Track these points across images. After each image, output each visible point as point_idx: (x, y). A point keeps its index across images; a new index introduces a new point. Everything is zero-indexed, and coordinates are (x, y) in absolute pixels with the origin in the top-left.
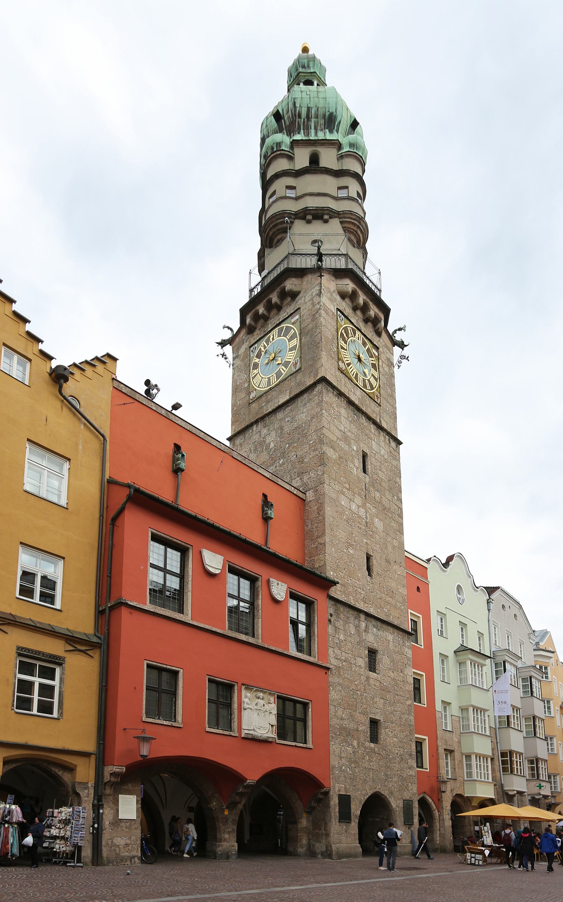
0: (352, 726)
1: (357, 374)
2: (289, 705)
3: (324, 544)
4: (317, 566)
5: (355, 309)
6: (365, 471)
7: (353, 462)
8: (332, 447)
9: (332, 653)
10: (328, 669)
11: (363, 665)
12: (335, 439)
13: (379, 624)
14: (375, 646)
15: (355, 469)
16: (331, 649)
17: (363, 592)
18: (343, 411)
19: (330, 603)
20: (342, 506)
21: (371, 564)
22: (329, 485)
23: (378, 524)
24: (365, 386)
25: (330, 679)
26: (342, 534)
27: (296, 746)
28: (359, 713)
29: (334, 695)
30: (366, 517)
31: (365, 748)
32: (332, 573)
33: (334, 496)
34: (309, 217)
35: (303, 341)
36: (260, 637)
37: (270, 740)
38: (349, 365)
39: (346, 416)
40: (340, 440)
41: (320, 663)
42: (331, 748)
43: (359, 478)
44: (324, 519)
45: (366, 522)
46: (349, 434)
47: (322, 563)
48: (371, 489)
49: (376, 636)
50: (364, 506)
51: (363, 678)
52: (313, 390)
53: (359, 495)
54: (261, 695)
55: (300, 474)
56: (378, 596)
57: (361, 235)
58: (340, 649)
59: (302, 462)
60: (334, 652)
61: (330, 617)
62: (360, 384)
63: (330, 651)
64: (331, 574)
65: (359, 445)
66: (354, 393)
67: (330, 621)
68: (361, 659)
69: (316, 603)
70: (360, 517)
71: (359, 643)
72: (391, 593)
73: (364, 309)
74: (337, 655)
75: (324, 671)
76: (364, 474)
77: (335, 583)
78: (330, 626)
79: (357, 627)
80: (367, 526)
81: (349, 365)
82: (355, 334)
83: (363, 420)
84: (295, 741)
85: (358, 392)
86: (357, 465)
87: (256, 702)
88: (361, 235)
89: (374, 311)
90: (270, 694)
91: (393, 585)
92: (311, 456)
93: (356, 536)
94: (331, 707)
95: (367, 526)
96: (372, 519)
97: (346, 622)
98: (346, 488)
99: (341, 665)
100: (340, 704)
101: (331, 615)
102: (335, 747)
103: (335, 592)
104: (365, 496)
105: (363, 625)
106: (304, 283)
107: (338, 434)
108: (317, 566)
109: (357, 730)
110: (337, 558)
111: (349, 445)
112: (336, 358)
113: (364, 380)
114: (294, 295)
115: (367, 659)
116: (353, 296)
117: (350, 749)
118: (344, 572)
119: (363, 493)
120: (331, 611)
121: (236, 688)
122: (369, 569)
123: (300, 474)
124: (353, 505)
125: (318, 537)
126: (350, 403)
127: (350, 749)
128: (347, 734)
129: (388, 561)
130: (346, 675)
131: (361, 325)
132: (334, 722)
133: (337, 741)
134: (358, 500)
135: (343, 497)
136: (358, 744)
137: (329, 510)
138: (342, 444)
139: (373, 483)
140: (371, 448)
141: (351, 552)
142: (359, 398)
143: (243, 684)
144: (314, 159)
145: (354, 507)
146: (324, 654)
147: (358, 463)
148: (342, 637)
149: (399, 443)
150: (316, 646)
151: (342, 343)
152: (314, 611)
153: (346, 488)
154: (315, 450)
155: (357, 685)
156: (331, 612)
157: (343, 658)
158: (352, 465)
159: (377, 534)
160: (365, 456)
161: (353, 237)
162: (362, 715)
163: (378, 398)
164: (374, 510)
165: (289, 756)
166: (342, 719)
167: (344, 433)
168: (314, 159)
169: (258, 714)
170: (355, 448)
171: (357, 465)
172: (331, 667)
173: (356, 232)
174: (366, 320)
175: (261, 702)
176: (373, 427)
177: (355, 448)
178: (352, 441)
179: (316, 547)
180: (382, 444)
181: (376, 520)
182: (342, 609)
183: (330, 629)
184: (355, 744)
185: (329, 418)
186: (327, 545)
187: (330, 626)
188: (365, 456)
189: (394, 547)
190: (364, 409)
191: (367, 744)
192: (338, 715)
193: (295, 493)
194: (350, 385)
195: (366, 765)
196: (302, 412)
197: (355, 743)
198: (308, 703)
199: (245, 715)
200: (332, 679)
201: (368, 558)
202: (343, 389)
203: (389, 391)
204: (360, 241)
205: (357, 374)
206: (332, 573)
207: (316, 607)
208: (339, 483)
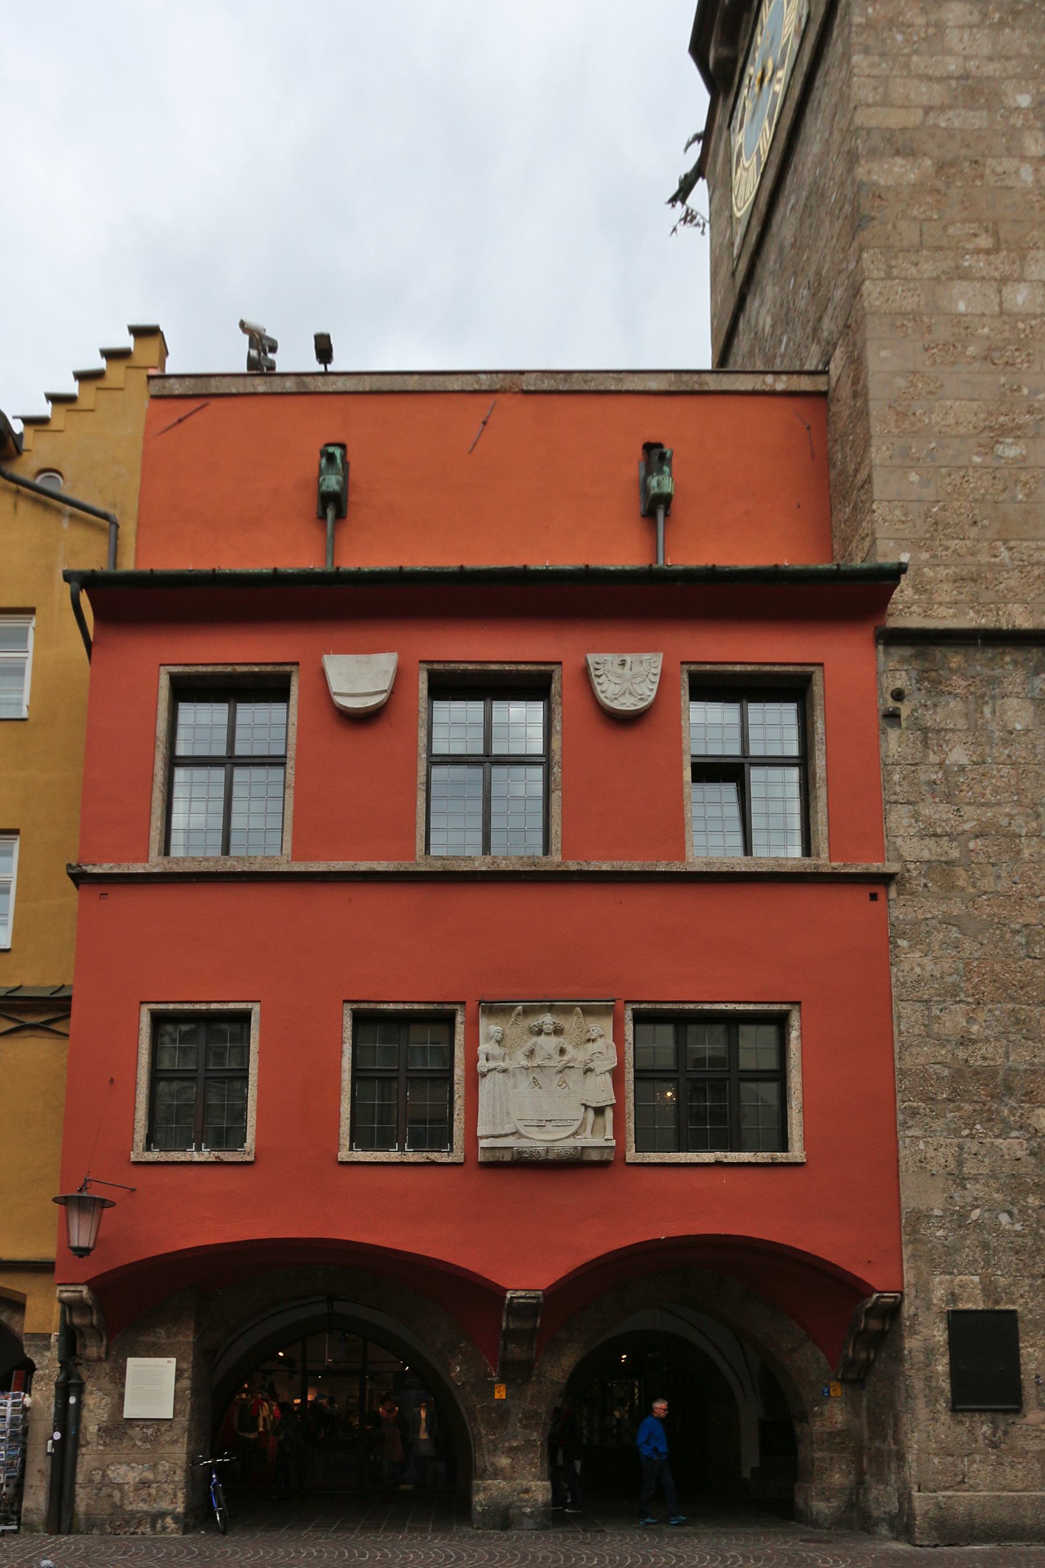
8: (898, 152)
9: (906, 822)
16: (904, 810)
22: (889, 276)
27: (718, 1164)
37: (595, 1156)
40: (942, 108)
42: (903, 1152)
58: (948, 798)
61: (891, 704)
67: (893, 716)
74: (932, 825)
75: (859, 895)
87: (528, 1046)
90: (587, 1012)
99: (955, 854)
103: (907, 610)
107: (936, 94)
120: (901, 680)
133: (938, 1125)
148: (958, 755)
152: (812, 707)
156: (899, 684)
157: (967, 827)
169: (535, 1081)
175: (548, 1043)
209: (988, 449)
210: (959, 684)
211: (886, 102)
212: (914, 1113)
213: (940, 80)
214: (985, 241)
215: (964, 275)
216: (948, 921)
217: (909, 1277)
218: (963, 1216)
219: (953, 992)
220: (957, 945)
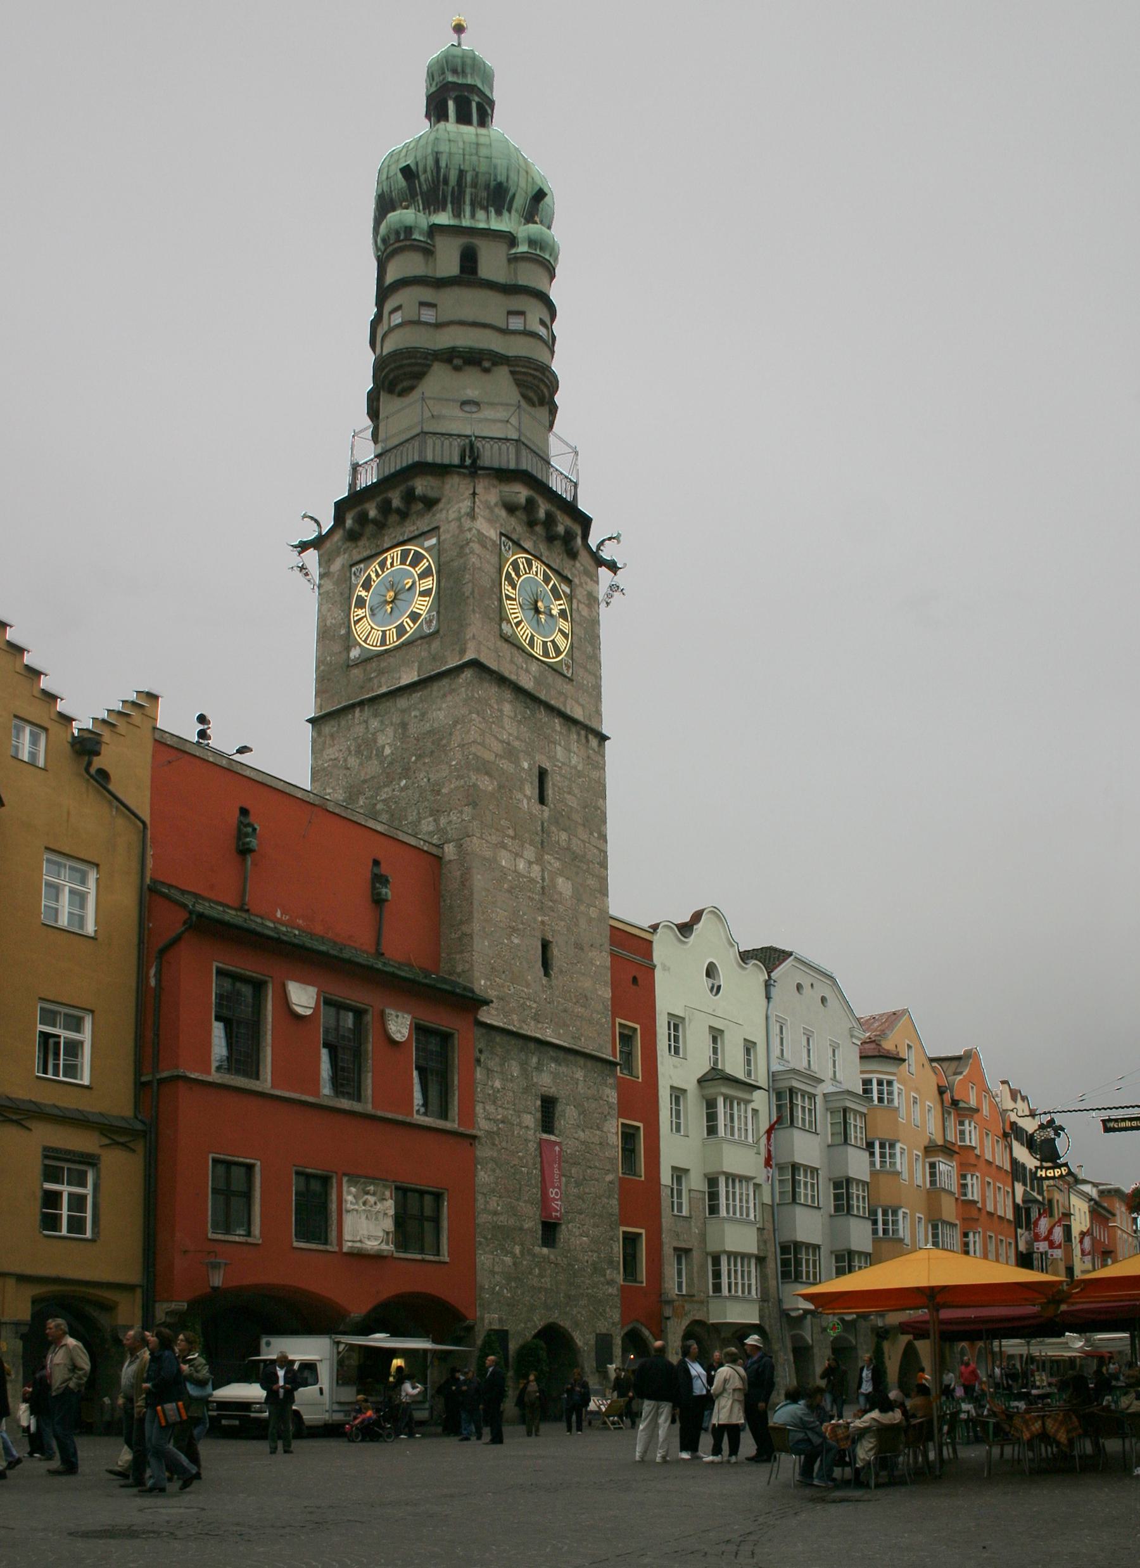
0: (512, 1222)
1: (532, 636)
2: (413, 1199)
3: (471, 936)
4: (459, 970)
5: (531, 524)
6: (542, 800)
7: (521, 789)
8: (487, 773)
10: (474, 1137)
11: (532, 1125)
12: (492, 758)
13: (561, 1055)
14: (553, 1091)
15: (525, 802)
17: (534, 1005)
18: (507, 708)
19: (479, 1032)
20: (501, 872)
21: (549, 955)
23: (564, 886)
24: (546, 653)
25: (478, 1153)
26: (500, 915)
28: (525, 1201)
29: (483, 1177)
30: (543, 879)
31: (534, 1255)
32: (483, 982)
33: (488, 854)
34: (458, 362)
35: (442, 584)
36: (370, 1100)
38: (518, 624)
39: (512, 714)
40: (501, 757)
41: (461, 1130)
43: (531, 814)
44: (472, 894)
45: (543, 888)
46: (516, 743)
47: (467, 966)
48: (553, 829)
49: (555, 1076)
50: (539, 860)
51: (532, 1146)
52: (458, 676)
53: (532, 843)
54: (372, 1188)
55: (435, 813)
56: (560, 1008)
57: (545, 390)
58: (494, 1103)
59: (438, 793)
60: (484, 1109)
62: (538, 651)
63: (479, 1109)
64: (481, 985)
65: (533, 758)
66: (527, 671)
68: (529, 1116)
69: (456, 1036)
70: (532, 880)
71: (526, 1090)
72: (583, 999)
73: (550, 521)
76: (540, 806)
77: (487, 1002)
78: (478, 1069)
79: (523, 1065)
80: (543, 893)
81: (518, 624)
82: (530, 567)
83: (542, 715)
84: (422, 1252)
85: (534, 667)
86: (528, 793)
88: (545, 390)
89: (563, 524)
91: (587, 984)
92: (452, 786)
93: (524, 914)
94: (479, 1197)
95: (543, 893)
96: (552, 880)
97: (504, 1059)
98: (509, 836)
100: (493, 1191)
101: (481, 1051)
102: (484, 1259)
103: (488, 1016)
104: (542, 842)
105: (535, 1060)
106: (447, 487)
108: (459, 970)
109: (521, 1229)
110: (492, 957)
111: (517, 762)
112: (497, 619)
113: (545, 643)
114: (430, 503)
115: (539, 1115)
116: (530, 502)
117: (508, 1260)
118: (503, 976)
119: (538, 839)
120: (481, 1045)
121: (334, 1180)
122: (546, 964)
123: (435, 813)
124: (522, 863)
125: (462, 923)
126: (518, 690)
127: (508, 1260)
128: (504, 1235)
129: (579, 946)
130: (504, 1144)
131: (542, 547)
132: (482, 1218)
133: (487, 1249)
134: (530, 853)
135: (503, 853)
136: (522, 1252)
137: (479, 880)
138: (505, 764)
139: (555, 820)
140: (552, 758)
141: (516, 941)
142: (534, 677)
143: (345, 1174)
144: (469, 259)
145: (522, 865)
146: (468, 1115)
147: (531, 790)
148: (497, 1084)
149: (603, 738)
150: (456, 1103)
151: (507, 589)
153: (509, 836)
154: (459, 777)
155: (521, 1159)
158: (520, 796)
159: (561, 903)
160: (542, 774)
161: (531, 394)
162: (529, 1205)
163: (568, 667)
164: (557, 864)
165: (416, 1277)
166: (495, 1213)
167: (508, 744)
168: (469, 259)
170: (526, 765)
171: (528, 793)
172: (479, 1133)
173: (538, 387)
174: (551, 538)
176: (557, 723)
177: (526, 765)
178: (521, 755)
179: (460, 939)
180: (574, 747)
181: (560, 880)
182: (498, 1039)
183: (479, 1074)
184: (517, 1252)
185: (483, 726)
186: (476, 939)
187: (478, 1069)
188: (542, 774)
189: (590, 920)
190: (543, 697)
191: (537, 1249)
192: (490, 1208)
193: (425, 848)
194: (519, 659)
195: (535, 1282)
196: (442, 708)
197: (517, 1250)
198: (442, 1194)
199: (348, 1221)
200: (483, 1152)
201: (545, 946)
202: (507, 671)
203: (589, 649)
204: (544, 396)
205: (532, 636)
206: (483, 982)
207: (456, 1042)
208: (497, 830)
209: (509, 939)
210: (499, 1050)
211: (483, 744)
212: (480, 1243)
213: (502, 742)
214: (511, 832)
215: (504, 846)
216: (492, 1159)
217: (478, 1314)
218: (494, 1289)
219: (493, 1191)
220: (494, 1171)
